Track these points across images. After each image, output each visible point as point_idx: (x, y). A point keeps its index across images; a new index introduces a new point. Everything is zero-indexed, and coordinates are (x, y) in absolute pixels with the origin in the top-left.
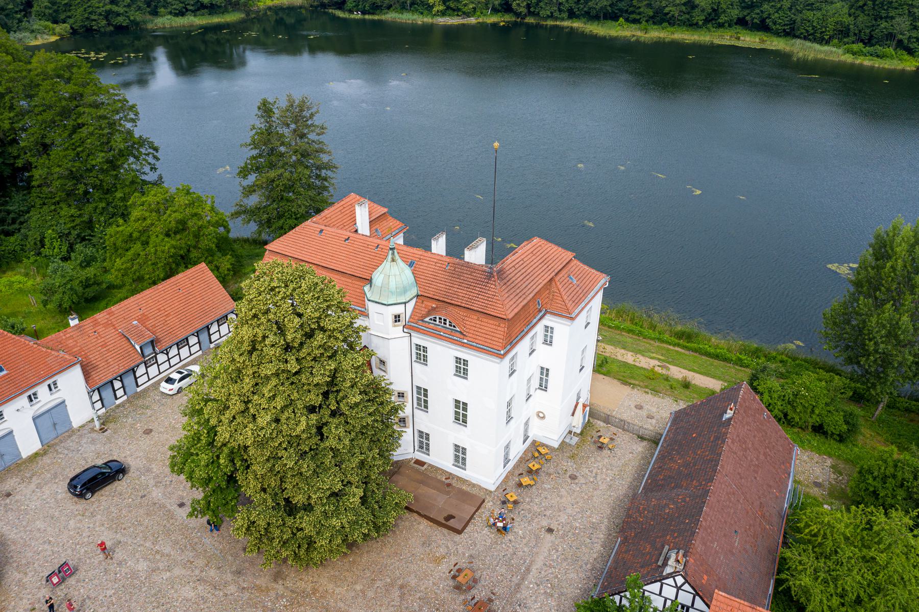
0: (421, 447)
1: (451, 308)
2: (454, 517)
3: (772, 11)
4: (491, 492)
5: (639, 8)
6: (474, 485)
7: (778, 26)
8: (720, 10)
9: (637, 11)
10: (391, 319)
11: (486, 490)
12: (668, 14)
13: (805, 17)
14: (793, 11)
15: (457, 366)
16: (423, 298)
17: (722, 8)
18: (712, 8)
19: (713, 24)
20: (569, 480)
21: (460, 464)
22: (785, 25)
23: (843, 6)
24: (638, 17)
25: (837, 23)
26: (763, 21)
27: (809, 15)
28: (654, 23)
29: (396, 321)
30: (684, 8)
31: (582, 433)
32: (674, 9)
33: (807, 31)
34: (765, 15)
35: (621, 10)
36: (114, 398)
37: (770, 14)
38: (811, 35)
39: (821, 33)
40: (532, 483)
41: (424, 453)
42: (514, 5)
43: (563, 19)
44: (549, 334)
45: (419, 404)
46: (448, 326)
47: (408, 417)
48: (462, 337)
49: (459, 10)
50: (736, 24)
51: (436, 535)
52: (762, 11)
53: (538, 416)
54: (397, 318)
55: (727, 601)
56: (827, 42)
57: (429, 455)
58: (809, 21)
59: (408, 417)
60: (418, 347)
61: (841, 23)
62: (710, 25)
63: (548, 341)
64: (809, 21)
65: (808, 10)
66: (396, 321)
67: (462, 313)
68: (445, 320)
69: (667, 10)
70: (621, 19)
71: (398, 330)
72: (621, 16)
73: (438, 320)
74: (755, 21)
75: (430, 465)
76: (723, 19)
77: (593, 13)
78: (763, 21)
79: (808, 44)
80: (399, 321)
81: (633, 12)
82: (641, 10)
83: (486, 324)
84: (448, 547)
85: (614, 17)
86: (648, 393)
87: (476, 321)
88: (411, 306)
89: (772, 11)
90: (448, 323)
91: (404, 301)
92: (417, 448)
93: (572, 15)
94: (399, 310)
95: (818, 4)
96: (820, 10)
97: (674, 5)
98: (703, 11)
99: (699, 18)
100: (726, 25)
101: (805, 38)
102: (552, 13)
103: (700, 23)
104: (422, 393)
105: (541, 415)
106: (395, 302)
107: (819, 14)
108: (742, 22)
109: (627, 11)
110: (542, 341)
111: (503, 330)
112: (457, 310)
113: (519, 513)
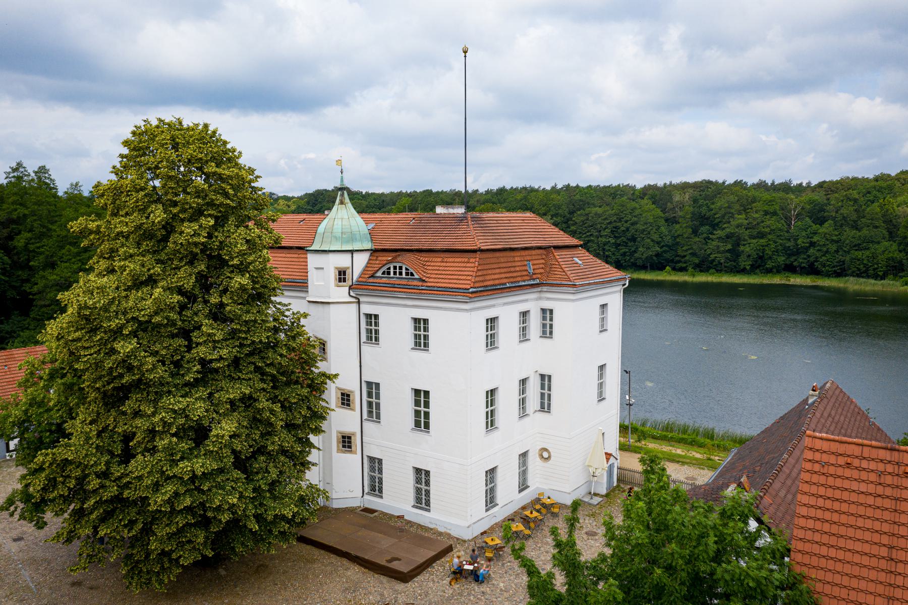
0: (373, 488)
1: (409, 255)
2: (400, 560)
3: (819, 254)
4: (465, 541)
5: (685, 256)
6: (441, 534)
7: (827, 268)
8: (766, 257)
9: (683, 260)
10: (332, 275)
11: (458, 539)
12: (713, 260)
13: (853, 257)
14: (840, 253)
15: (416, 335)
16: (377, 254)
17: (767, 254)
18: (757, 254)
19: (760, 271)
20: (585, 537)
21: (423, 505)
22: (834, 267)
23: (891, 245)
24: (684, 265)
25: (888, 259)
26: (812, 265)
27: (859, 254)
28: (701, 271)
29: (340, 281)
30: (728, 255)
31: (607, 495)
32: (719, 255)
33: (859, 269)
34: (812, 259)
36: (5, 450)
37: (817, 258)
38: (863, 272)
39: (874, 269)
40: (527, 532)
41: (376, 496)
44: (548, 322)
45: (370, 413)
46: (404, 276)
47: (354, 434)
48: (420, 284)
50: (784, 270)
51: (369, 582)
52: (809, 256)
53: (542, 457)
54: (342, 275)
55: (834, 447)
56: (883, 278)
57: (381, 497)
58: (859, 260)
59: (354, 434)
60: (369, 316)
61: (893, 259)
62: (758, 271)
63: (547, 331)
64: (859, 260)
65: (856, 250)
66: (340, 281)
67: (423, 257)
68: (401, 268)
69: (713, 256)
70: (668, 268)
71: (342, 293)
73: (392, 271)
74: (803, 265)
75: (383, 513)
76: (770, 264)
77: (640, 263)
78: (812, 265)
79: (862, 280)
80: (345, 281)
81: (680, 262)
82: (687, 258)
83: (452, 264)
84: (382, 595)
85: (660, 268)
86: (703, 469)
87: (439, 264)
88: (361, 260)
89: (819, 254)
90: (404, 271)
91: (351, 249)
92: (366, 490)
94: (343, 261)
95: (865, 244)
96: (868, 249)
97: (718, 252)
98: (749, 256)
99: (746, 263)
100: (775, 270)
101: (859, 276)
103: (748, 268)
104: (373, 389)
105: (545, 455)
106: (340, 249)
107: (867, 253)
108: (790, 269)
109: (672, 261)
110: (539, 333)
111: (472, 265)
112: (418, 255)
113: (503, 565)
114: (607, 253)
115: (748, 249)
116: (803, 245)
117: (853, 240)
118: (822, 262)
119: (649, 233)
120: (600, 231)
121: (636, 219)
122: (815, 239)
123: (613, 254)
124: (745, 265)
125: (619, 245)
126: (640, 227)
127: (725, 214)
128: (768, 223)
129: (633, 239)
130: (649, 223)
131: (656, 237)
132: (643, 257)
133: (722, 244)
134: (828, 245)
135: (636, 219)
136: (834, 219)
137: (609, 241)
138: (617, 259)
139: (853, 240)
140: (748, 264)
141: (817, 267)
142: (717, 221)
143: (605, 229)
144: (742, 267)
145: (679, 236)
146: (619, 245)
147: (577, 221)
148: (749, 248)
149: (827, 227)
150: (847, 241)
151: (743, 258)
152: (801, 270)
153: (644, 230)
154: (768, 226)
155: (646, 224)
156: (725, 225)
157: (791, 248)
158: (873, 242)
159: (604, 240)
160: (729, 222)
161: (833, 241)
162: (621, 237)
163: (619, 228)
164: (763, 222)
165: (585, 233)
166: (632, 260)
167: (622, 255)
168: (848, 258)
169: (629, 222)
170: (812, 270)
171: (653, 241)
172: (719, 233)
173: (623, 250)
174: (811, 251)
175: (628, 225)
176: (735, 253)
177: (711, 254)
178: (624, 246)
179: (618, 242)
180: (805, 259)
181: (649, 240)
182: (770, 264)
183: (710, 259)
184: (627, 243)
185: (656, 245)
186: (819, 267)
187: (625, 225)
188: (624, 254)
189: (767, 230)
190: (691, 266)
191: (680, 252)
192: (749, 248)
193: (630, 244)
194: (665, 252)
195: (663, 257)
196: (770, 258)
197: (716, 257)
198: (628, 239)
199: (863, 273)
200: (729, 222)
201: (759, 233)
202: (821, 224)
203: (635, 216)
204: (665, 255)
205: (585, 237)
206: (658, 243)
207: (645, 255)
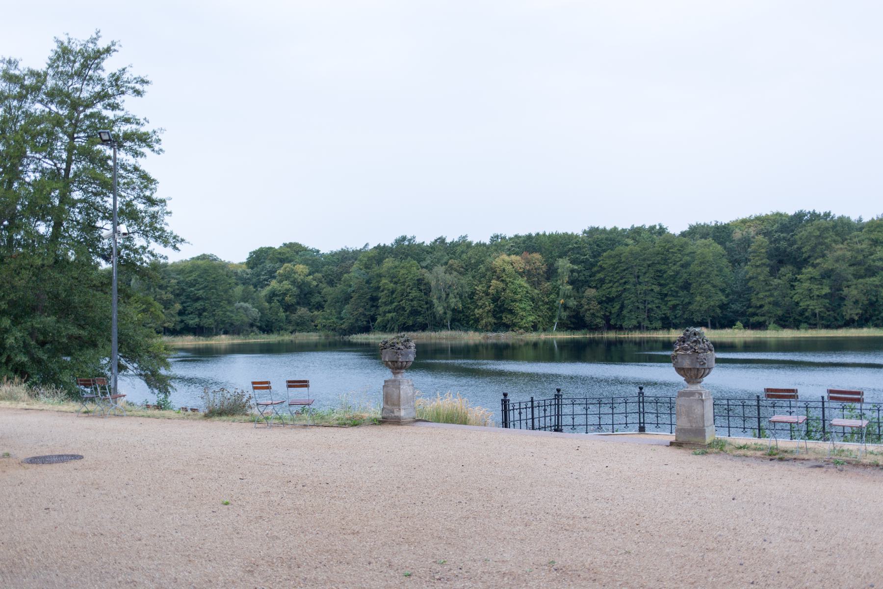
5: (761, 306)
12: (805, 310)
24: (761, 319)
35: (735, 312)
42: (588, 318)
43: (655, 329)
49: (514, 325)
69: (803, 304)
72: (737, 320)
81: (754, 314)
82: (766, 308)
98: (856, 302)
102: (639, 323)
109: (743, 314)
114: (650, 306)
115: (855, 292)
119: (708, 276)
120: (638, 277)
121: (688, 258)
123: (658, 307)
124: (851, 315)
125: (666, 295)
126: (695, 268)
127: (816, 245)
129: (686, 286)
131: (718, 281)
132: (702, 308)
133: (817, 287)
137: (652, 290)
138: (664, 314)
140: (857, 312)
142: (805, 256)
143: (645, 273)
144: (847, 317)
145: (751, 278)
146: (666, 295)
147: (605, 266)
151: (849, 303)
153: (701, 273)
156: (818, 261)
159: (645, 288)
160: (823, 256)
162: (668, 284)
163: (665, 272)
164: (871, 254)
165: (618, 281)
166: (685, 316)
171: (714, 286)
172: (808, 271)
173: (673, 302)
175: (676, 268)
176: (836, 299)
178: (673, 296)
181: (709, 286)
183: (800, 308)
184: (677, 292)
185: (720, 294)
187: (673, 268)
188: (674, 307)
190: (772, 320)
192: (852, 292)
193: (681, 293)
194: (733, 301)
195: (731, 308)
197: (808, 306)
200: (823, 256)
201: (866, 270)
203: (688, 255)
204: (733, 306)
205: (617, 287)
207: (705, 307)
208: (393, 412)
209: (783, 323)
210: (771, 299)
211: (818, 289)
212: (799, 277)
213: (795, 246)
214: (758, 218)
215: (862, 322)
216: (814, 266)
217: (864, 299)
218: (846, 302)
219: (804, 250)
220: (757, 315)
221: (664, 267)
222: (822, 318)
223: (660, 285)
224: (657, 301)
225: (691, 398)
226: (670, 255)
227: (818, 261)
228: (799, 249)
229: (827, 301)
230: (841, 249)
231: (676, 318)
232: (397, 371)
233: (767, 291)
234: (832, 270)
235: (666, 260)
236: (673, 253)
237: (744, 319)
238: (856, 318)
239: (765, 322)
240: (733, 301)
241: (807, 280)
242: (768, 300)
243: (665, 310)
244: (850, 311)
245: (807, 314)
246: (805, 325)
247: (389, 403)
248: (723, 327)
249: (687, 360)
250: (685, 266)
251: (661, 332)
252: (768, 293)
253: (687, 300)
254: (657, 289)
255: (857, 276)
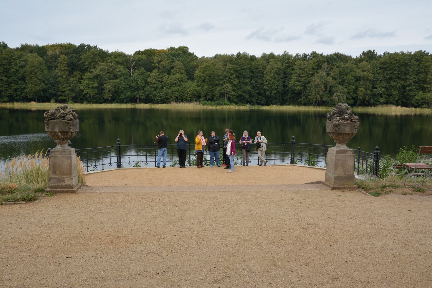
9: (63, 94)
12: (86, 94)
24: (65, 98)
32: (90, 90)
34: (147, 93)
43: (5, 102)
61: (195, 90)
69: (85, 91)
81: (60, 95)
82: (67, 92)
89: (152, 89)
93: (12, 100)
98: (109, 91)
100: (125, 101)
109: (55, 95)
115: (109, 86)
116: (142, 84)
117: (171, 80)
118: (154, 94)
121: (24, 63)
122: (149, 80)
124: (107, 97)
125: (11, 83)
128: (119, 69)
129: (23, 78)
130: (35, 66)
131: (41, 77)
133: (92, 83)
134: (156, 83)
135: (24, 63)
136: (158, 68)
138: (10, 93)
139: (171, 80)
141: (151, 98)
142: (86, 67)
144: (106, 98)
145: (59, 77)
148: (108, 86)
149: (154, 73)
150: (168, 82)
152: (139, 101)
153: (32, 72)
154: (120, 71)
155: (33, 66)
156: (92, 70)
157: (134, 86)
158: (183, 81)
161: (159, 81)
162: (12, 77)
166: (23, 95)
167: (14, 91)
168: (170, 91)
169: (18, 65)
170: (148, 100)
171: (39, 80)
172: (88, 75)
174: (148, 87)
176: (100, 89)
177: (84, 89)
178: (15, 84)
179: (10, 80)
180: (143, 93)
181: (36, 79)
182: (122, 97)
183: (84, 93)
184: (17, 82)
185: (42, 84)
186: (152, 97)
188: (16, 90)
189: (120, 73)
190: (70, 99)
191: (61, 89)
192: (108, 86)
193: (20, 82)
194: (49, 88)
196: (122, 92)
197: (88, 92)
198: (18, 78)
199: (180, 99)
200: (95, 68)
202: (151, 71)
203: (23, 61)
206: (44, 82)
207: (34, 90)
208: (64, 181)
209: (76, 100)
210: (69, 88)
211: (92, 84)
212: (83, 77)
213: (81, 62)
214: (60, 45)
215: (111, 101)
216: (91, 72)
217: (113, 90)
218: (105, 91)
219: (85, 64)
220: (62, 96)
221: (9, 67)
222: (94, 98)
223: (7, 77)
224: (5, 86)
225: (345, 154)
226: (13, 60)
227: (92, 70)
228: (83, 63)
229: (96, 90)
230: (103, 65)
231: (17, 96)
232: (64, 142)
233: (67, 84)
234: (99, 75)
235: (10, 63)
236: (14, 59)
237: (56, 98)
238: (109, 99)
239: (66, 99)
240: (49, 88)
241: (87, 79)
242: (68, 88)
243: (10, 91)
244: (107, 95)
245: (87, 96)
246: (86, 102)
247: (57, 173)
248: (44, 101)
249: (348, 128)
250: (22, 67)
251: (8, 103)
252: (68, 85)
253: (23, 86)
254: (5, 79)
255: (110, 79)
